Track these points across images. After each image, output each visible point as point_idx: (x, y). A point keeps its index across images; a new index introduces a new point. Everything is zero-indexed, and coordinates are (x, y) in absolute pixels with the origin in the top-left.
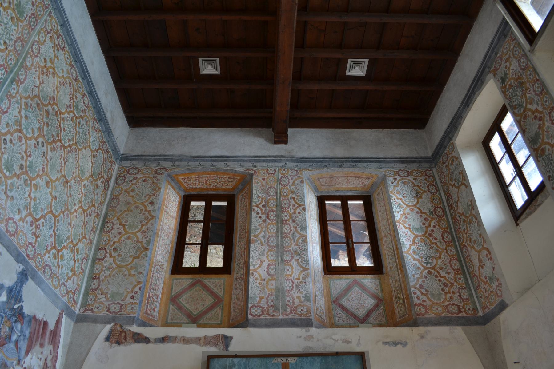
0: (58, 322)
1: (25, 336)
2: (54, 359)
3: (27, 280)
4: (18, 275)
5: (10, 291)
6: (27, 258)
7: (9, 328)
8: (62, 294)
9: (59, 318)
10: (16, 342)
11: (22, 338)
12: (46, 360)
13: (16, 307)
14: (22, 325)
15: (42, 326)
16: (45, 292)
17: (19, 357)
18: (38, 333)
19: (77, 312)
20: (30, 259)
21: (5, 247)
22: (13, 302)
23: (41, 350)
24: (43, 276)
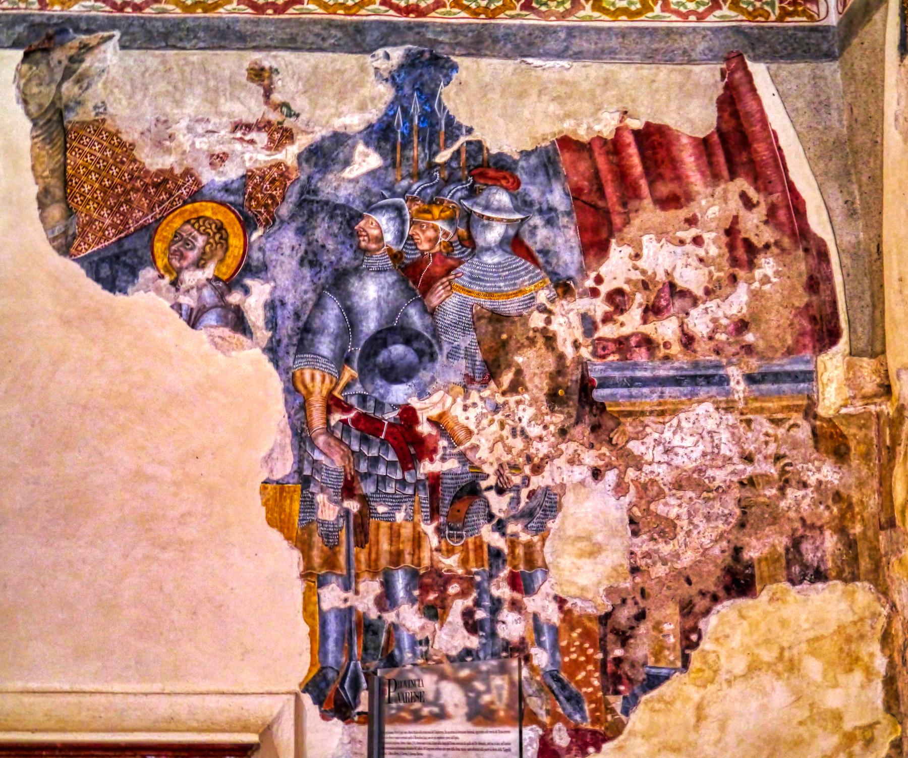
0: (735, 101)
1: (551, 209)
2: (782, 215)
3: (454, 67)
4: (392, 79)
5: (381, 134)
6: (412, 18)
7: (451, 220)
8: (685, 16)
9: (727, 87)
10: (515, 244)
11: (537, 220)
12: (731, 232)
13: (443, 157)
14: (513, 186)
15: (633, 150)
16: (578, 56)
17: (553, 274)
18: (622, 175)
19: (833, 20)
20: (421, 13)
21: (276, 48)
22: (416, 151)
23: (683, 213)
24: (532, 20)
